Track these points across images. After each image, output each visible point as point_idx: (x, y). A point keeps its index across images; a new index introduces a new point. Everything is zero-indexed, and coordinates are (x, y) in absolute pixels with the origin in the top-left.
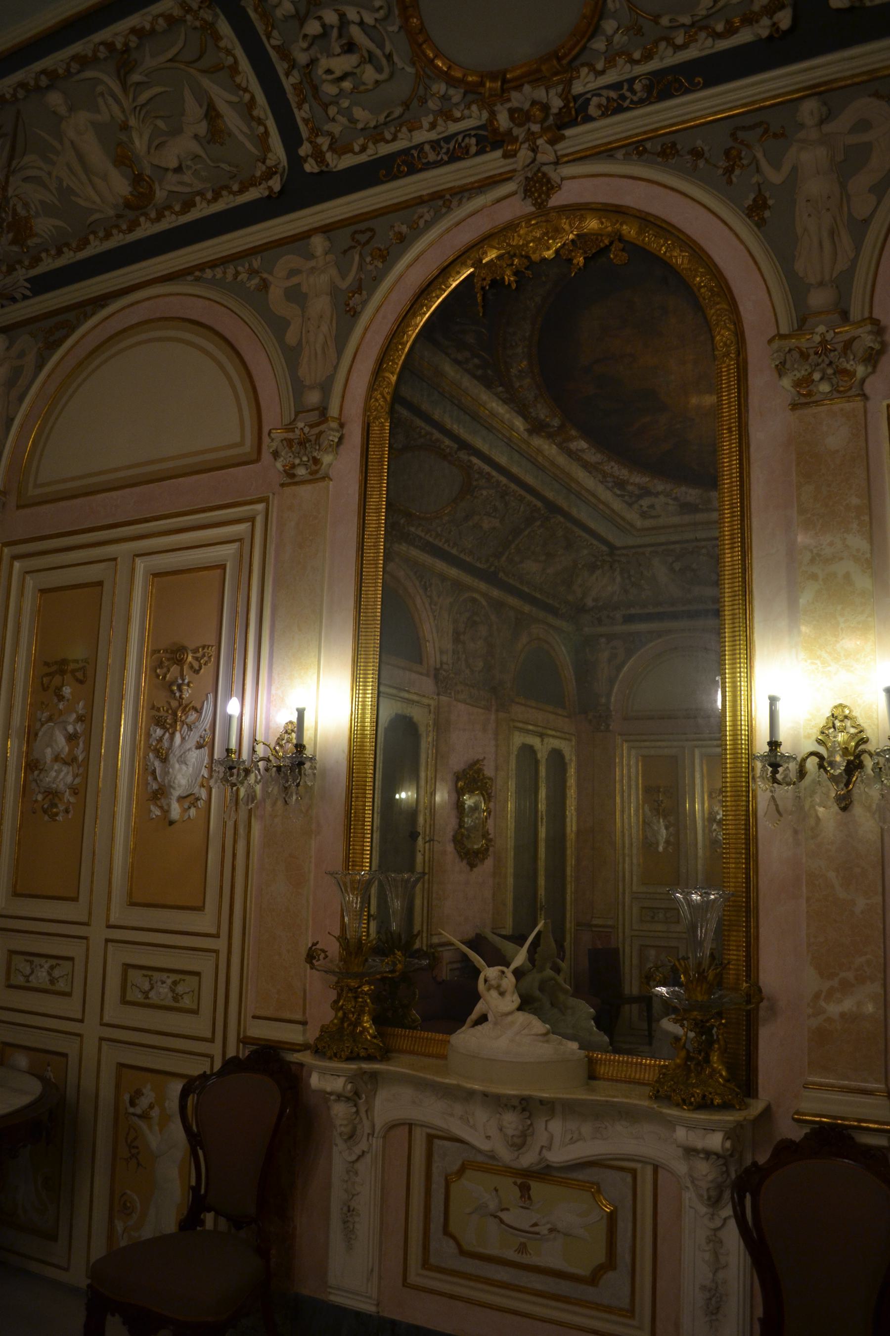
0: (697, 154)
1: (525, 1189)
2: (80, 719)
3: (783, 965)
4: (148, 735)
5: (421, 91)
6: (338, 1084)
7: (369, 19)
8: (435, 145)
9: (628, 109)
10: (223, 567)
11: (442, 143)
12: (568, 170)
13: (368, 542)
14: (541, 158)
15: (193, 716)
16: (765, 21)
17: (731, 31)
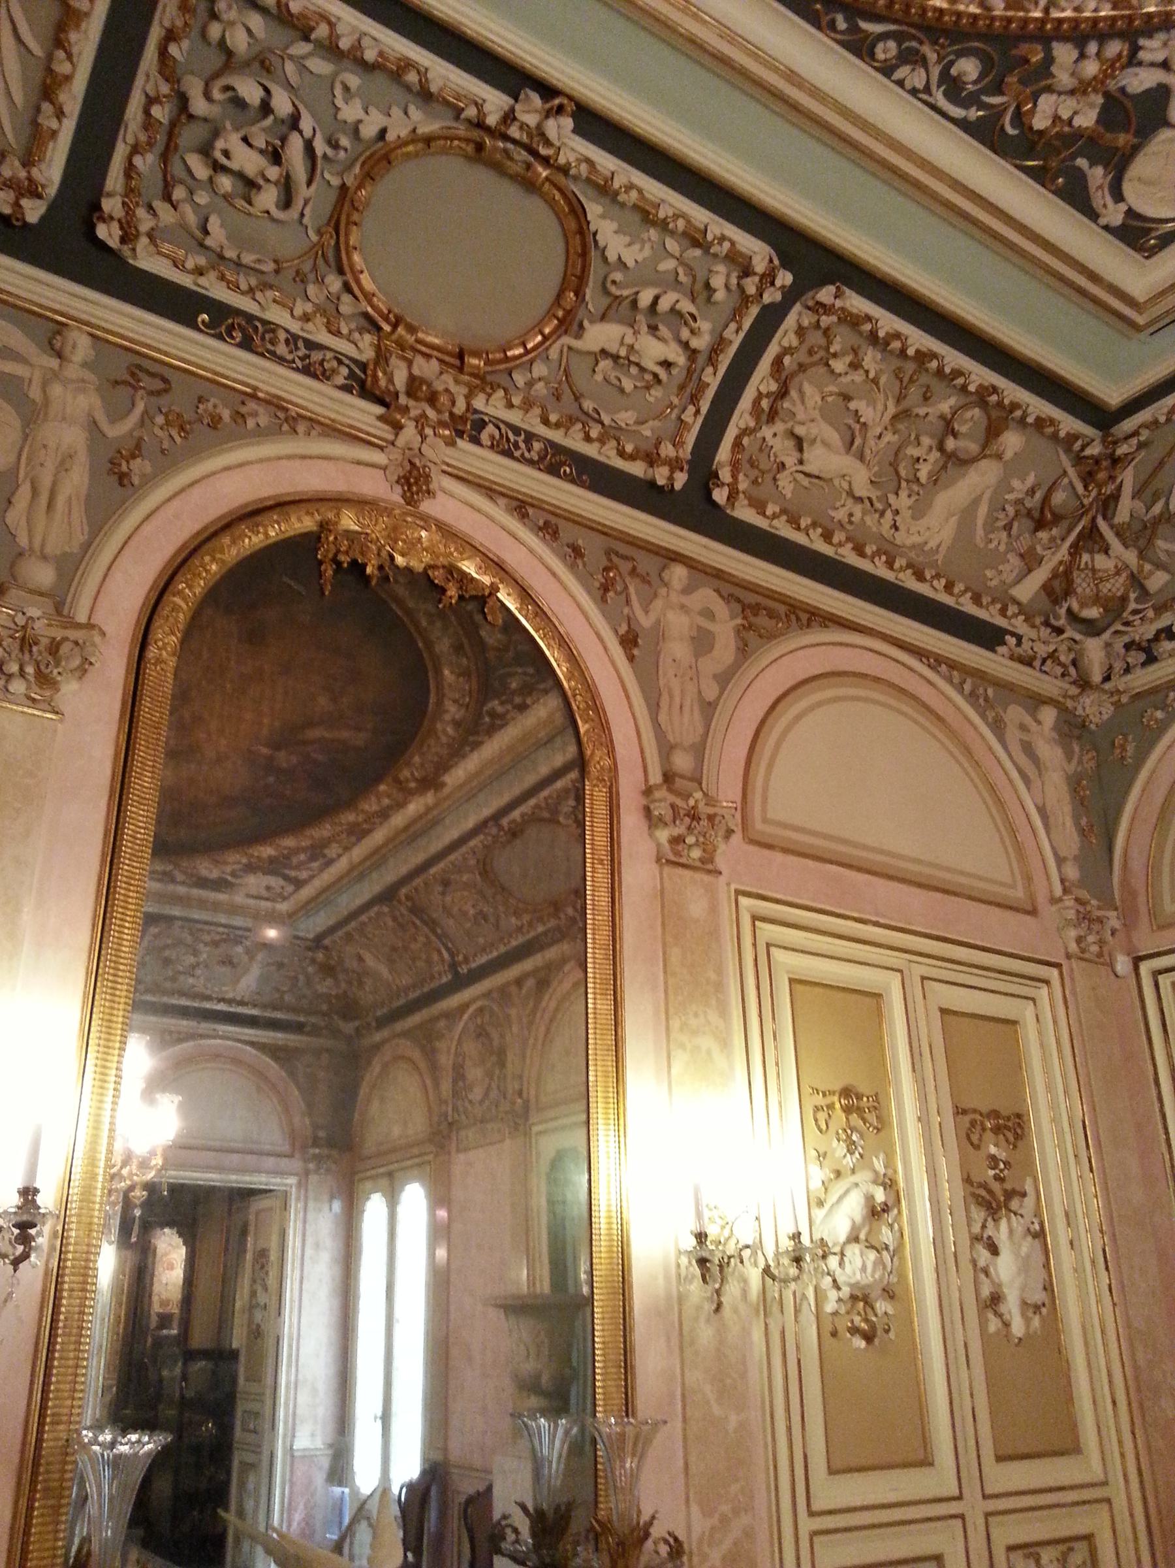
0: (577, 551)
5: (307, 267)
7: (320, 147)
8: (293, 340)
11: (300, 344)
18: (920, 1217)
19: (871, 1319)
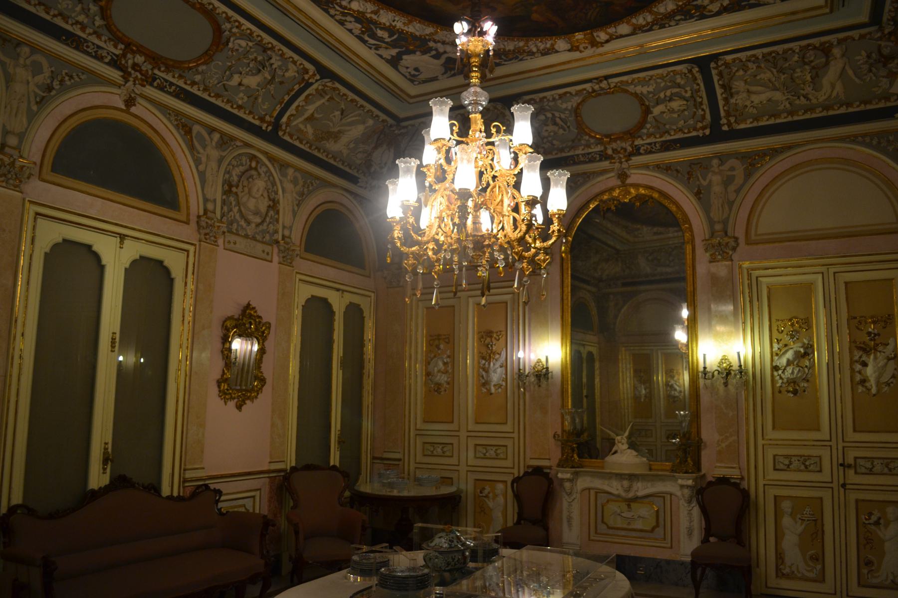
0: (677, 171)
1: (629, 506)
2: (449, 357)
3: (709, 433)
4: (479, 363)
6: (568, 476)
7: (563, 116)
8: (583, 155)
9: (654, 152)
10: (507, 303)
12: (632, 171)
13: (565, 297)
14: (624, 166)
15: (497, 356)
16: (701, 131)
17: (689, 132)
18: (821, 356)
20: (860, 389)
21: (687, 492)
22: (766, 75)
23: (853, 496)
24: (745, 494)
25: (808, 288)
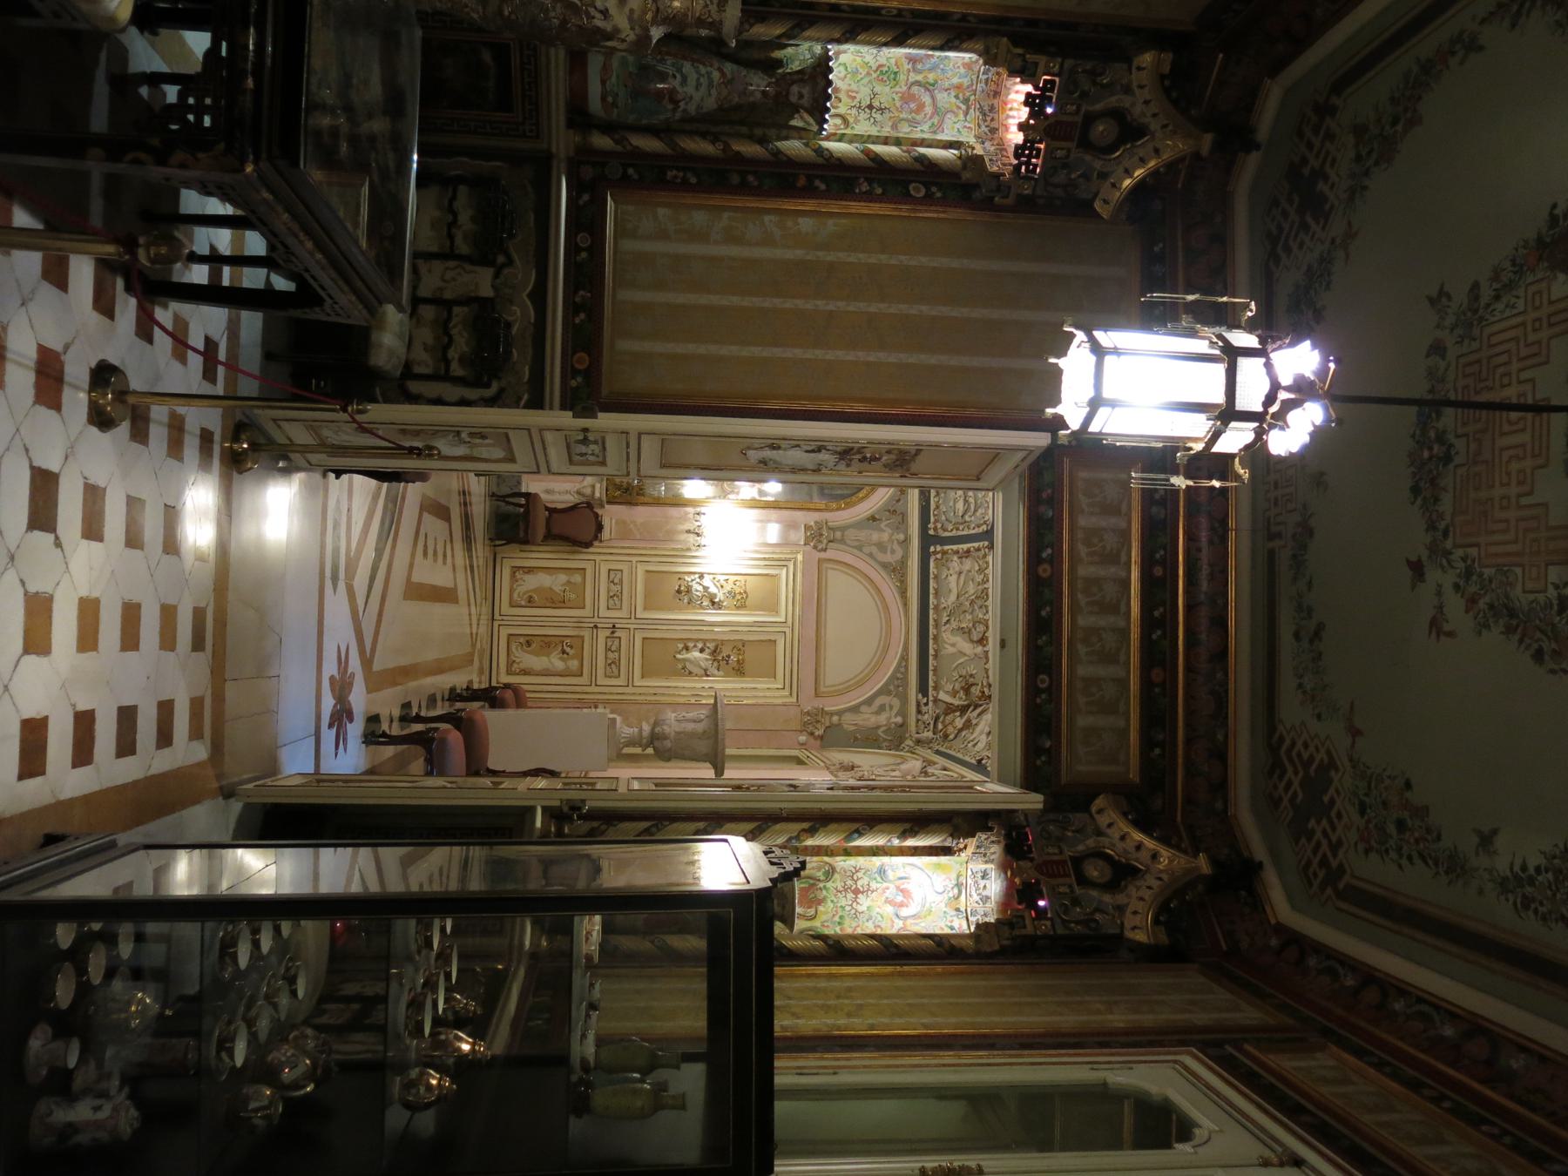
3: (641, 514)
19: (683, 593)
20: (681, 646)
21: (588, 491)
22: (971, 589)
23: (586, 634)
24: (588, 545)
25: (774, 609)
